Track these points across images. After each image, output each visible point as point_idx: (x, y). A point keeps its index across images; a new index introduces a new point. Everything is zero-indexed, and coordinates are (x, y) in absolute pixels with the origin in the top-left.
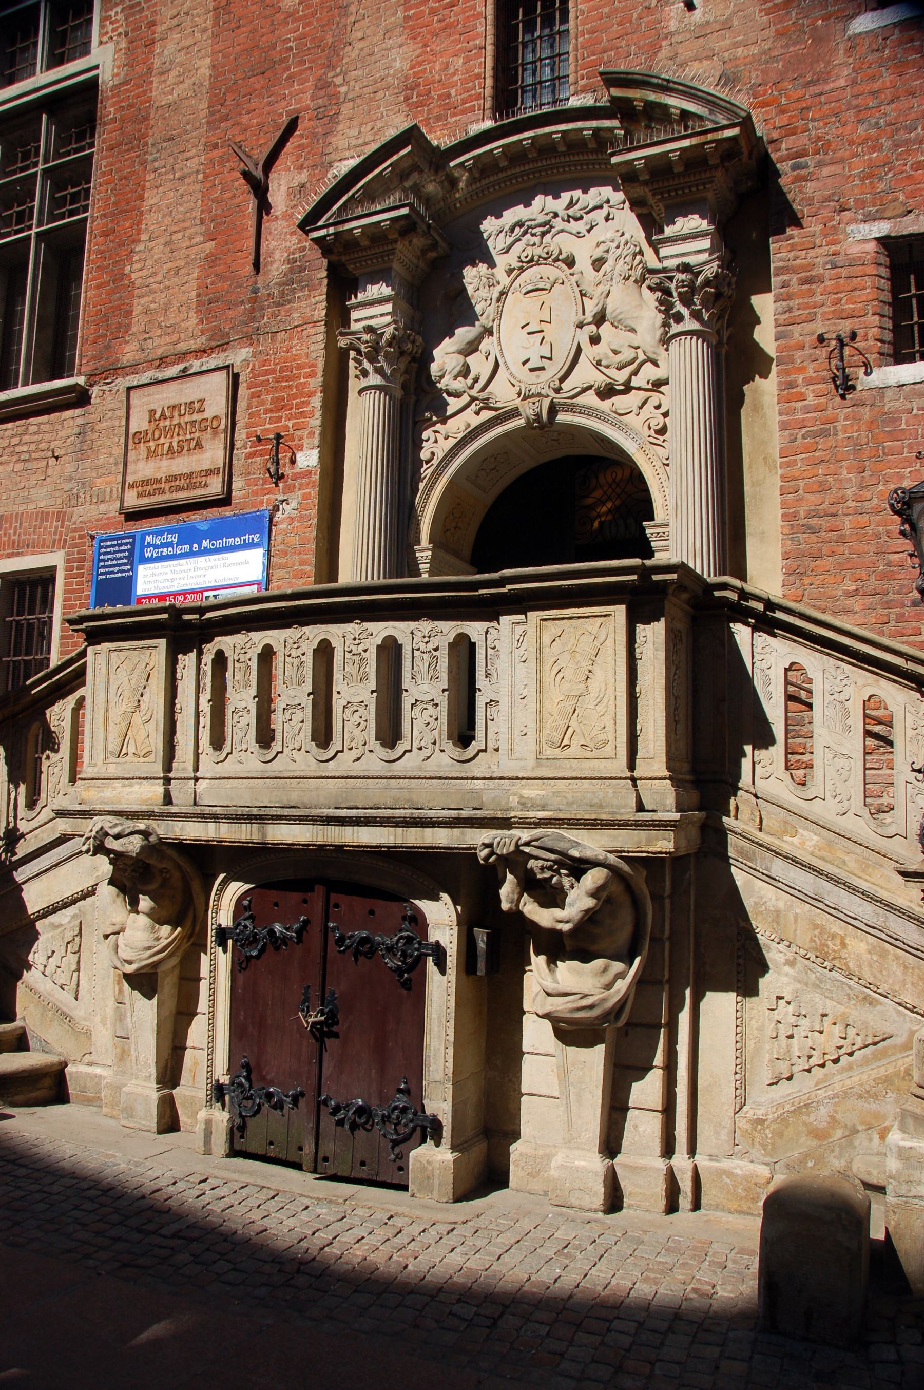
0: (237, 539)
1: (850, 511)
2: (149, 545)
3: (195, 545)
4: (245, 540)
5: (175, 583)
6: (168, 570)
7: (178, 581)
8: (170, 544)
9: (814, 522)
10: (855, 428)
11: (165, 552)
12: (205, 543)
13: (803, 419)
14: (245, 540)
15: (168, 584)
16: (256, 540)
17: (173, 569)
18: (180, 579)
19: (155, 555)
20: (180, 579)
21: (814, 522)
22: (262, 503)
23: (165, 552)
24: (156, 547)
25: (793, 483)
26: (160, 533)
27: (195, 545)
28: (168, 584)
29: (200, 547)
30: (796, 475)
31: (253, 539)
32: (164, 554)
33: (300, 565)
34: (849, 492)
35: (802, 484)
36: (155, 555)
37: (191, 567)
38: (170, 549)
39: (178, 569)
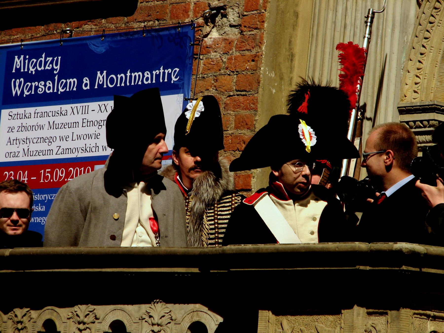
0: (147, 74)
2: (19, 74)
3: (86, 80)
4: (158, 76)
5: (54, 146)
6: (43, 121)
7: (58, 143)
8: (46, 75)
11: (42, 87)
12: (101, 77)
14: (158, 76)
15: (44, 146)
16: (174, 79)
17: (51, 119)
18: (61, 139)
19: (26, 93)
20: (61, 139)
22: (186, 11)
23: (42, 87)
24: (29, 77)
26: (33, 52)
27: (86, 80)
28: (44, 146)
29: (93, 81)
31: (169, 75)
32: (40, 91)
33: (237, 128)
36: (26, 93)
37: (78, 118)
38: (49, 84)
39: (59, 120)
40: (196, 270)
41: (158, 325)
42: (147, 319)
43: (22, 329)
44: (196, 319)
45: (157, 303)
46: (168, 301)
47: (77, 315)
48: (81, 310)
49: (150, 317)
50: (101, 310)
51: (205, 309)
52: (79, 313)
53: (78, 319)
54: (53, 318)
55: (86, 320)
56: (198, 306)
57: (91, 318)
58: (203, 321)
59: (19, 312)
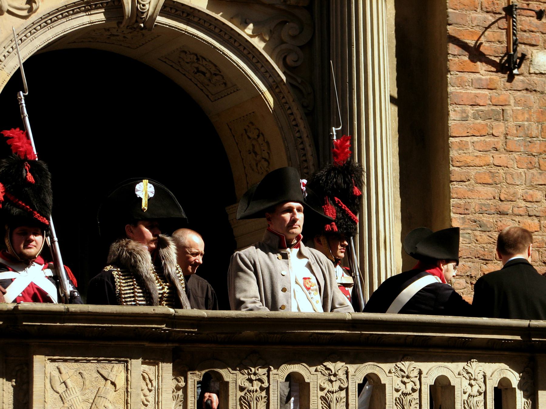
1: (522, 211)
9: (485, 218)
10: (526, 116)
13: (476, 96)
21: (485, 218)
25: (465, 170)
30: (468, 160)
34: (520, 191)
35: (473, 172)
40: (518, 338)
41: (475, 379)
42: (465, 374)
43: (336, 381)
44: (502, 376)
45: (473, 362)
46: (480, 360)
47: (402, 370)
48: (406, 365)
49: (468, 373)
50: (424, 366)
51: (507, 367)
52: (403, 368)
53: (403, 373)
54: (376, 372)
55: (411, 375)
56: (503, 366)
57: (416, 373)
58: (508, 377)
59: (329, 365)
